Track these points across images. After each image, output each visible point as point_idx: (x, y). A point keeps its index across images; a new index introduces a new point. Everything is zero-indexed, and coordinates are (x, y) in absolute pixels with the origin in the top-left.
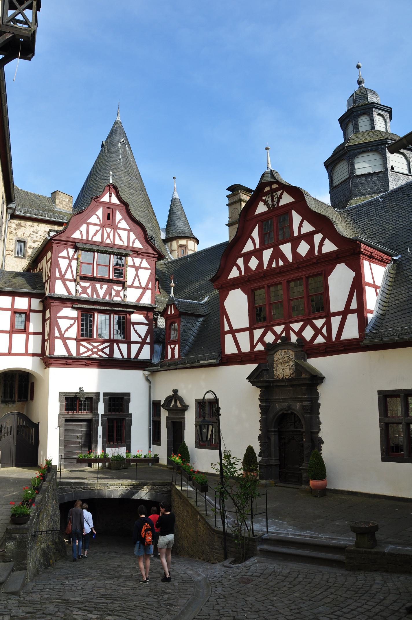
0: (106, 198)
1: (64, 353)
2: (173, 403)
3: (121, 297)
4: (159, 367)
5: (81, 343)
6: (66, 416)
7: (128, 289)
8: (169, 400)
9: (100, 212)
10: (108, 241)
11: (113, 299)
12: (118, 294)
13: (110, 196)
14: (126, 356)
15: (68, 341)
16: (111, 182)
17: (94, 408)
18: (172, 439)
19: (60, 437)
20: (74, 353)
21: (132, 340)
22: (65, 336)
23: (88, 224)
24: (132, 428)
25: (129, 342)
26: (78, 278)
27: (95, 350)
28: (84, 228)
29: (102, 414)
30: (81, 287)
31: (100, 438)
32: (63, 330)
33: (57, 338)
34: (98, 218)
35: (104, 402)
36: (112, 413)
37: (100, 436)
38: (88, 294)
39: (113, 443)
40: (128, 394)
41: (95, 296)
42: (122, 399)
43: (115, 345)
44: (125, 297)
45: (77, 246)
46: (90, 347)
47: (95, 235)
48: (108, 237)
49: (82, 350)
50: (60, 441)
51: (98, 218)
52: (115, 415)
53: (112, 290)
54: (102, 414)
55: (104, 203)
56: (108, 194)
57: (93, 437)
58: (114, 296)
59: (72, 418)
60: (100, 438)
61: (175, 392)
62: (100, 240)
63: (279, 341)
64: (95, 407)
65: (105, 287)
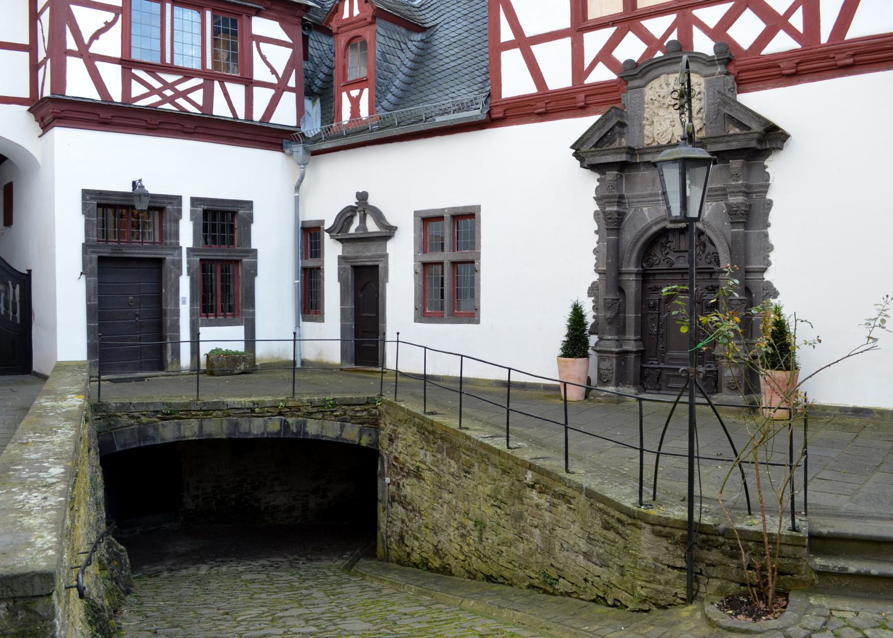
1: (91, 93)
5: (134, 71)
8: (346, 217)
14: (241, 115)
15: (99, 65)
22: (92, 50)
25: (249, 83)
27: (169, 93)
29: (188, 249)
33: (72, 53)
35: (191, 219)
39: (216, 316)
43: (217, 84)
46: (157, 85)
52: (218, 253)
54: (188, 249)
60: (184, 303)
63: (659, 54)
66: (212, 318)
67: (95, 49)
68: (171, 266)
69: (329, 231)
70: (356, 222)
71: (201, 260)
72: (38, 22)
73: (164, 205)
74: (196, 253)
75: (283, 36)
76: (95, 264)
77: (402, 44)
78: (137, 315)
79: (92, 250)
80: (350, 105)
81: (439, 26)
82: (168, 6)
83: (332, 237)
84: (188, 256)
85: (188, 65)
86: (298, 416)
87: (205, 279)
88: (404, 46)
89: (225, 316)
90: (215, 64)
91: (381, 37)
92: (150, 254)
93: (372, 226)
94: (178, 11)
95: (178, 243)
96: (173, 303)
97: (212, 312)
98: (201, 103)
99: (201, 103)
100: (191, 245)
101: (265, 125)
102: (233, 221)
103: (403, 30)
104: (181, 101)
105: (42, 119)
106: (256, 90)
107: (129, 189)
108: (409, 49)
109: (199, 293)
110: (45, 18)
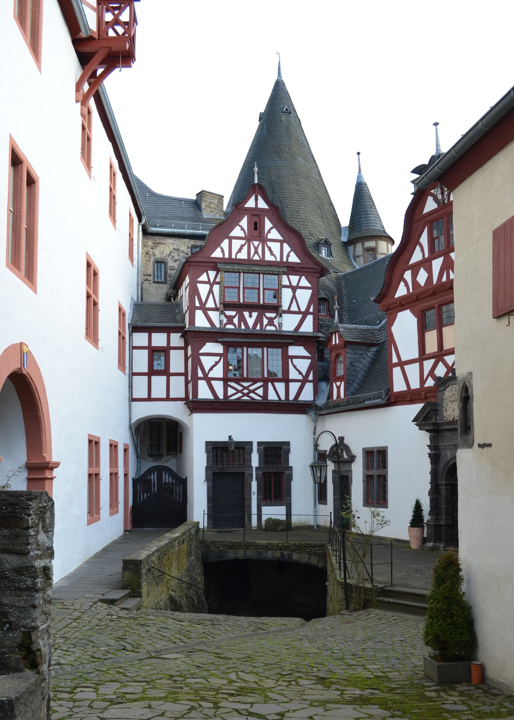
0: (250, 204)
5: (229, 383)
9: (244, 222)
10: (256, 258)
11: (265, 329)
12: (271, 322)
13: (256, 200)
15: (213, 382)
16: (256, 182)
20: (221, 396)
22: (209, 376)
23: (231, 239)
26: (222, 306)
27: (246, 391)
28: (225, 244)
29: (256, 467)
30: (226, 316)
34: (242, 229)
35: (258, 452)
38: (234, 325)
41: (243, 327)
44: (281, 325)
45: (218, 267)
46: (240, 388)
47: (239, 251)
48: (256, 252)
49: (231, 391)
51: (242, 229)
54: (256, 467)
55: (250, 209)
56: (253, 198)
58: (266, 325)
62: (246, 257)
65: (255, 314)
67: (211, 375)
73: (244, 446)
95: (251, 465)
98: (262, 395)
99: (262, 395)
100: (257, 466)
104: (252, 395)
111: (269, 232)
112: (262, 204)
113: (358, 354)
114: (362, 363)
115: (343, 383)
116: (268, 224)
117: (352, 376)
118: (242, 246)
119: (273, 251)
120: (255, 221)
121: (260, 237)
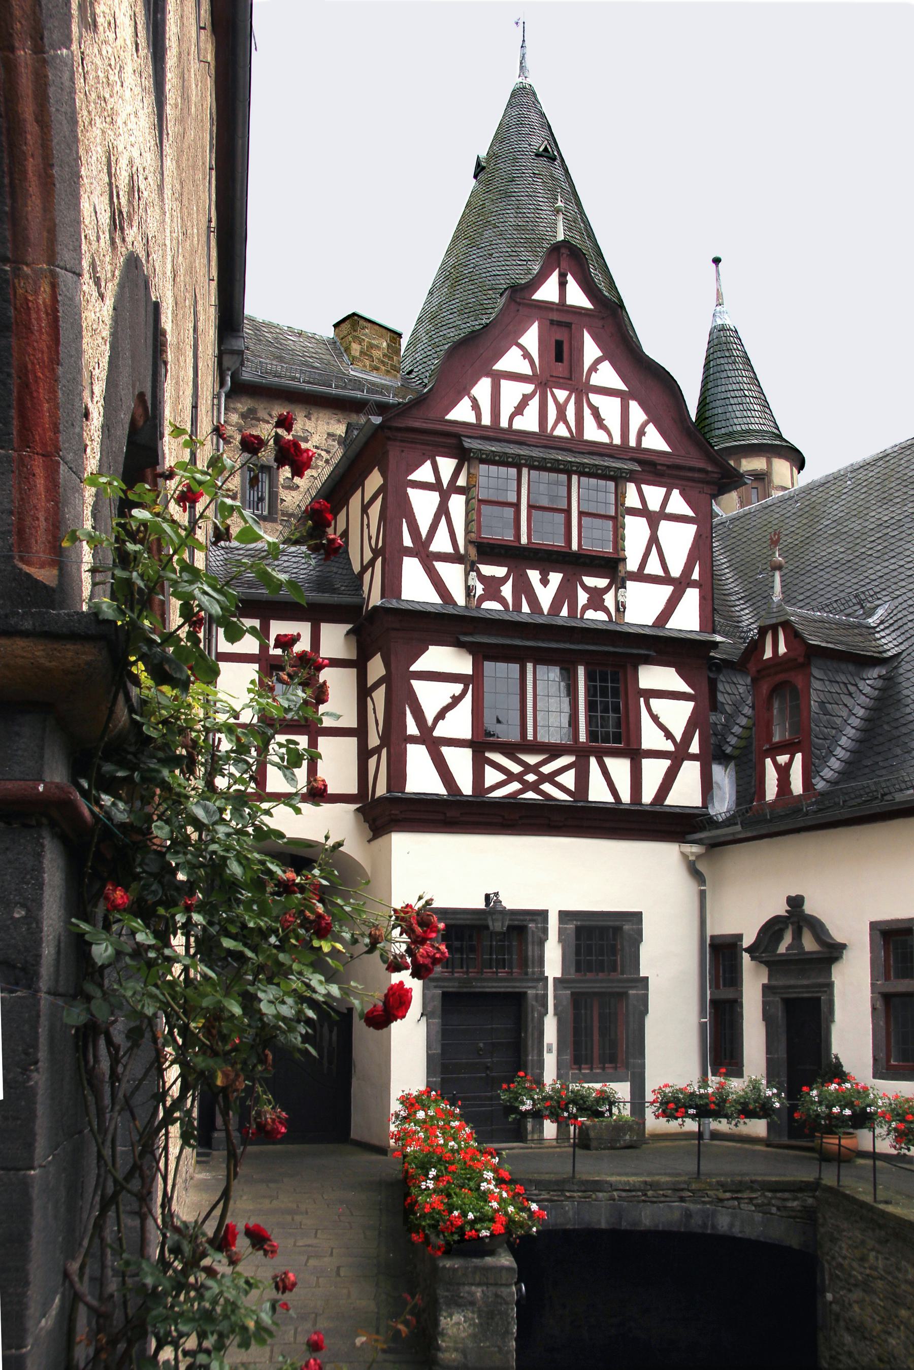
0: (548, 292)
1: (434, 786)
2: (787, 940)
3: (606, 611)
4: (738, 828)
6: (446, 984)
7: (629, 584)
9: (531, 338)
10: (561, 431)
12: (596, 599)
13: (563, 284)
14: (626, 797)
15: (446, 751)
16: (561, 237)
17: (530, 957)
18: (782, 1054)
19: (429, 1047)
20: (466, 787)
21: (646, 745)
22: (436, 733)
24: (650, 1022)
26: (473, 552)
27: (531, 778)
30: (482, 578)
31: (550, 1051)
32: (430, 716)
34: (527, 355)
35: (560, 940)
36: (585, 975)
37: (550, 1046)
39: (591, 1069)
40: (636, 917)
42: (617, 930)
43: (593, 761)
45: (466, 445)
46: (516, 769)
48: (561, 416)
49: (492, 776)
50: (430, 1058)
51: (527, 355)
52: (596, 982)
53: (580, 589)
55: (545, 306)
56: (554, 278)
57: (530, 1049)
58: (585, 608)
59: (465, 990)
60: (550, 1051)
61: (795, 902)
62: (534, 427)
64: (533, 956)
65: (555, 578)
66: (587, 1071)
67: (441, 731)
68: (534, 1003)
69: (748, 950)
70: (787, 939)
71: (573, 994)
72: (369, 699)
73: (525, 923)
74: (565, 985)
75: (682, 686)
76: (438, 1003)
77: (849, 686)
78: (488, 1068)
79: (435, 984)
80: (776, 776)
81: (905, 654)
82: (530, 666)
83: (753, 958)
84: (555, 990)
85: (555, 739)
86: (704, 1203)
87: (577, 1019)
88: (852, 689)
89: (603, 1068)
90: (592, 735)
91: (818, 682)
92: (508, 987)
93: (809, 944)
94: (541, 669)
95: (543, 972)
96: (535, 1052)
97: (586, 1064)
98: (572, 787)
99: (572, 787)
100: (559, 975)
101: (657, 808)
102: (615, 939)
103: (851, 668)
104: (547, 787)
105: (374, 820)
106: (646, 763)
107: (480, 904)
108: (861, 691)
109: (570, 1038)
110: (379, 695)
111: (594, 368)
112: (577, 297)
113: (838, 682)
114: (846, 705)
115: (799, 757)
116: (591, 350)
117: (825, 739)
118: (526, 400)
119: (603, 417)
120: (558, 338)
121: (570, 379)
